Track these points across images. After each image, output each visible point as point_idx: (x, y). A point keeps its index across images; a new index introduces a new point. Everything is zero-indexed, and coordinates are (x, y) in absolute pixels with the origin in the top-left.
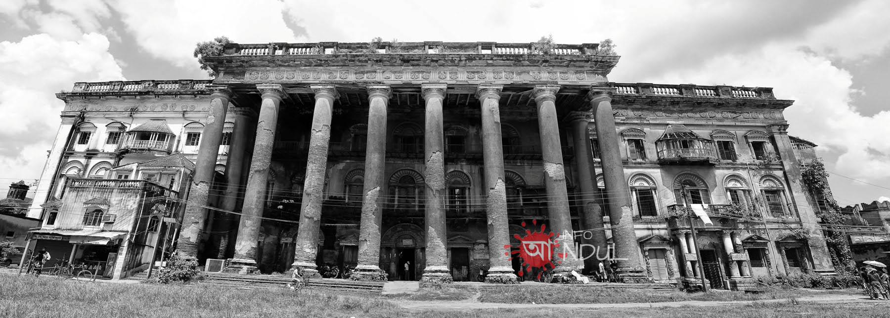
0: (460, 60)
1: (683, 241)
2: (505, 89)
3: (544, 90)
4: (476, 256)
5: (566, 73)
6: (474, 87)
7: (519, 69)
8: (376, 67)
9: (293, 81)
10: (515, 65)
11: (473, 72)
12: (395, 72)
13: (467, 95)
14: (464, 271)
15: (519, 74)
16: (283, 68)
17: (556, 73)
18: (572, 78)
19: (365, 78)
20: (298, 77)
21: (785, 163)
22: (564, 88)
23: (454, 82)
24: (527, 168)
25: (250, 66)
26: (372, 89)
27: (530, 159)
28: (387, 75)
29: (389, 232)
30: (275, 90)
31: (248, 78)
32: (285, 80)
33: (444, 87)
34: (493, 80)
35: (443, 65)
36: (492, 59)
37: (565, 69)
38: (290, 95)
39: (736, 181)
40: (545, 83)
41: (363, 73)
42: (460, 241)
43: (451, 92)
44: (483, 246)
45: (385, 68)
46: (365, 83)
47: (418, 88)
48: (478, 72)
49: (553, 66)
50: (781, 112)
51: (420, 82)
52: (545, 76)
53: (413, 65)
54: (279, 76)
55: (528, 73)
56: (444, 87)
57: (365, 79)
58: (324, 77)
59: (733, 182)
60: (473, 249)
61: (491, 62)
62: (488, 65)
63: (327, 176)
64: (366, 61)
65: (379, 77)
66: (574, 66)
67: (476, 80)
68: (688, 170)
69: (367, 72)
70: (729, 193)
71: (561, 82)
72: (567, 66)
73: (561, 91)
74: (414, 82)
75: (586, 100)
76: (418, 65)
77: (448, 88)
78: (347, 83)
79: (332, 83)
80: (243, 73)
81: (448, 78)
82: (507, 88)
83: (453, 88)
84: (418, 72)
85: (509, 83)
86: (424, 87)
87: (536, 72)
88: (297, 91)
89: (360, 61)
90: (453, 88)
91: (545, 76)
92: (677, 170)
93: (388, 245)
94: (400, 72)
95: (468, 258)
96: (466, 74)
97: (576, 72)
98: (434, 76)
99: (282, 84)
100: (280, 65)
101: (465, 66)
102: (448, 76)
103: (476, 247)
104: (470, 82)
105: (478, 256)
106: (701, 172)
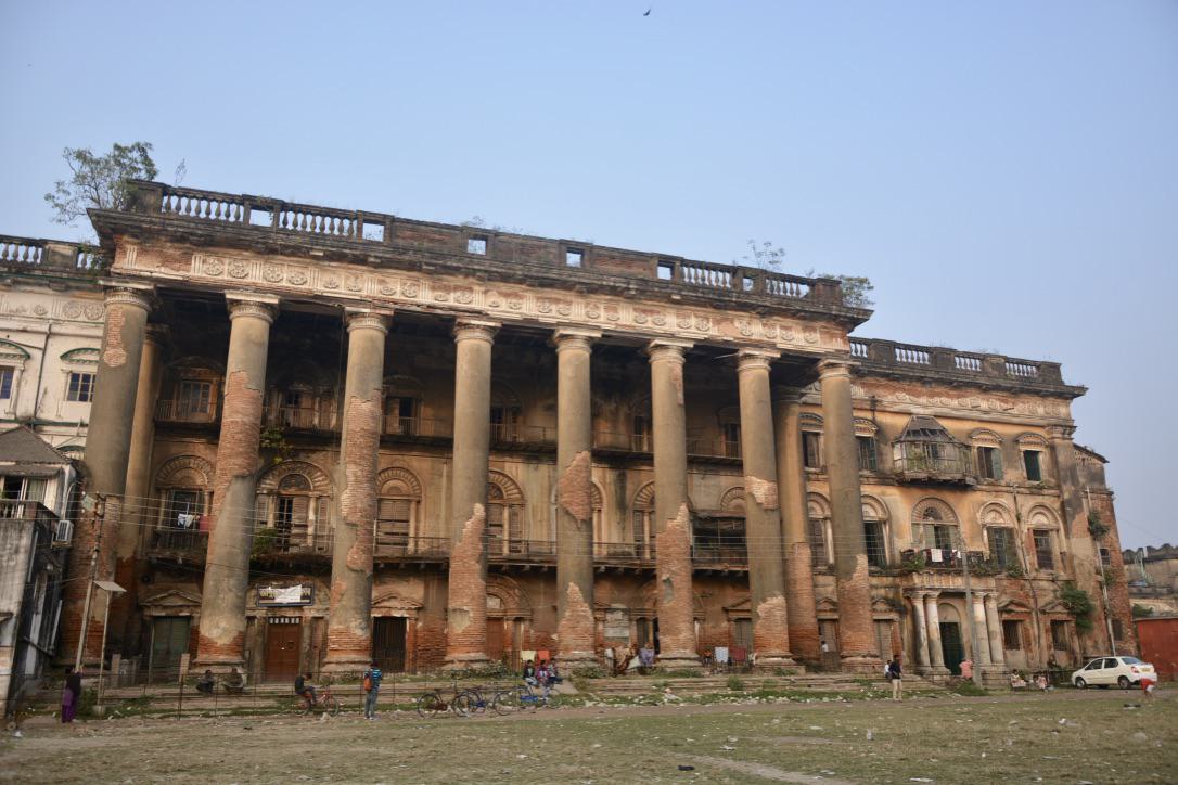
1: (919, 606)
11: (645, 311)
12: (507, 295)
19: (452, 300)
21: (1064, 487)
22: (786, 354)
23: (612, 327)
26: (467, 326)
31: (202, 269)
33: (597, 335)
34: (675, 329)
39: (997, 511)
40: (757, 345)
43: (605, 342)
44: (619, 615)
50: (1068, 405)
51: (554, 321)
59: (993, 515)
68: (932, 493)
70: (985, 533)
74: (542, 320)
77: (603, 336)
79: (383, 303)
85: (702, 337)
91: (755, 329)
92: (918, 494)
94: (516, 295)
103: (609, 616)
106: (950, 497)
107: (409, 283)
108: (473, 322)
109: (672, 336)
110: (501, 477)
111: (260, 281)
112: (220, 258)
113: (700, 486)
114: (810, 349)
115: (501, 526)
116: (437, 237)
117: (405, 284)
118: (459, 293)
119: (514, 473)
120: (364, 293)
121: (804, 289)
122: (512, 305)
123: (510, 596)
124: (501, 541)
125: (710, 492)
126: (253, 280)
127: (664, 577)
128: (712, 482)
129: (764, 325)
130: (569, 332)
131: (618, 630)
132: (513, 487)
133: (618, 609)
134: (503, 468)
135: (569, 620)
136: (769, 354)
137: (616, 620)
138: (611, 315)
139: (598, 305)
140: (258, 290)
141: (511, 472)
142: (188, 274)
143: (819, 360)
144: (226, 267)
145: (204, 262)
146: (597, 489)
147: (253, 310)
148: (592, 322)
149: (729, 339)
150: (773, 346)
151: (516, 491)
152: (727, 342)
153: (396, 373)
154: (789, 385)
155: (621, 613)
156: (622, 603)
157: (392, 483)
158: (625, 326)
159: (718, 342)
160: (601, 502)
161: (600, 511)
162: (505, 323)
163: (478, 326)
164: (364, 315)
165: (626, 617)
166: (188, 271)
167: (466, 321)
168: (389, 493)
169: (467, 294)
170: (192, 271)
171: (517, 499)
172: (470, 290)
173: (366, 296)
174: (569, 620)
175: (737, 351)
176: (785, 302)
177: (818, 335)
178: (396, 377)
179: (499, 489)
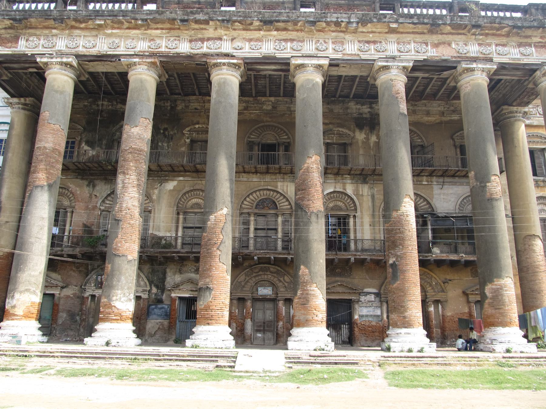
0: (349, 23)
2: (414, 69)
3: (472, 70)
4: (366, 311)
5: (504, 45)
6: (369, 64)
7: (435, 38)
8: (221, 32)
9: (94, 51)
10: (431, 32)
11: (368, 42)
12: (250, 40)
13: (356, 77)
14: (345, 330)
15: (436, 45)
16: (77, 32)
17: (490, 45)
18: (512, 53)
19: (205, 48)
20: (100, 44)
22: (502, 67)
23: (339, 56)
24: (436, 190)
25: (26, 27)
26: (216, 65)
27: (442, 176)
28: (237, 44)
29: (242, 277)
30: (66, 64)
32: (81, 50)
34: (396, 53)
35: (321, 31)
36: (396, 21)
37: (504, 40)
38: (91, 74)
40: (475, 60)
41: (202, 40)
42: (340, 289)
43: (335, 72)
44: (372, 297)
45: (235, 33)
46: (205, 55)
47: (285, 64)
48: (374, 42)
49: (487, 35)
51: (288, 56)
52: (473, 49)
53: (277, 30)
54: (72, 44)
55: (449, 44)
56: (326, 62)
57: (205, 50)
58: (142, 46)
60: (358, 301)
61: (394, 25)
62: (393, 31)
63: (148, 196)
64: (206, 22)
65: (226, 47)
66: (518, 34)
67: (371, 53)
69: (209, 39)
71: (498, 59)
72: (508, 35)
73: (496, 73)
74: (278, 55)
75: (531, 86)
76: (285, 29)
77: (331, 65)
78: (178, 55)
79: (152, 55)
80: (16, 39)
81: (330, 50)
82: (418, 66)
83: (337, 65)
84: (286, 40)
85: (421, 57)
86: (294, 62)
87: (461, 43)
88: (100, 68)
89: (197, 22)
90: (337, 65)
91: (473, 49)
93: (240, 295)
94: (258, 40)
95: (351, 315)
96: (357, 45)
97: (520, 45)
98: (309, 47)
99: (77, 56)
100: (73, 27)
101: (355, 32)
102: (331, 46)
103: (363, 298)
104: (363, 57)
105: (364, 311)
107: (172, 39)
108: (219, 61)
109: (394, 58)
110: (275, 194)
111: (64, 48)
112: (38, 37)
113: (440, 194)
114: (526, 61)
115: (276, 229)
116: (197, 6)
117: (169, 40)
118: (210, 43)
119: (285, 191)
120: (138, 49)
121: (518, 15)
122: (253, 47)
123: (280, 281)
124: (276, 240)
125: (448, 199)
126: (59, 49)
127: (391, 262)
128: (451, 191)
129: (480, 45)
130: (299, 61)
131: (371, 309)
132: (284, 200)
133: (371, 293)
134: (277, 187)
135: (300, 298)
136: (488, 66)
137: (369, 301)
138: (339, 47)
139: (327, 41)
140: (61, 54)
141: (283, 190)
142: (16, 49)
143: (535, 71)
144: (42, 42)
145: (27, 40)
146: (352, 199)
147: (58, 66)
148: (320, 54)
149: (446, 58)
150: (491, 60)
151: (287, 203)
152: (445, 60)
153: (198, 123)
154: (511, 105)
155: (373, 296)
156: (373, 287)
157: (194, 201)
158: (352, 55)
159: (438, 62)
160: (356, 210)
161: (355, 217)
162: (248, 61)
163: (224, 64)
164: (135, 64)
165: (378, 299)
166: (16, 48)
167: (215, 61)
168: (192, 207)
169: (218, 42)
170: (19, 47)
171: (287, 209)
172: (220, 39)
173: (139, 52)
174: (300, 298)
175: (455, 68)
176: (497, 20)
177: (533, 49)
178: (197, 126)
179: (274, 202)
